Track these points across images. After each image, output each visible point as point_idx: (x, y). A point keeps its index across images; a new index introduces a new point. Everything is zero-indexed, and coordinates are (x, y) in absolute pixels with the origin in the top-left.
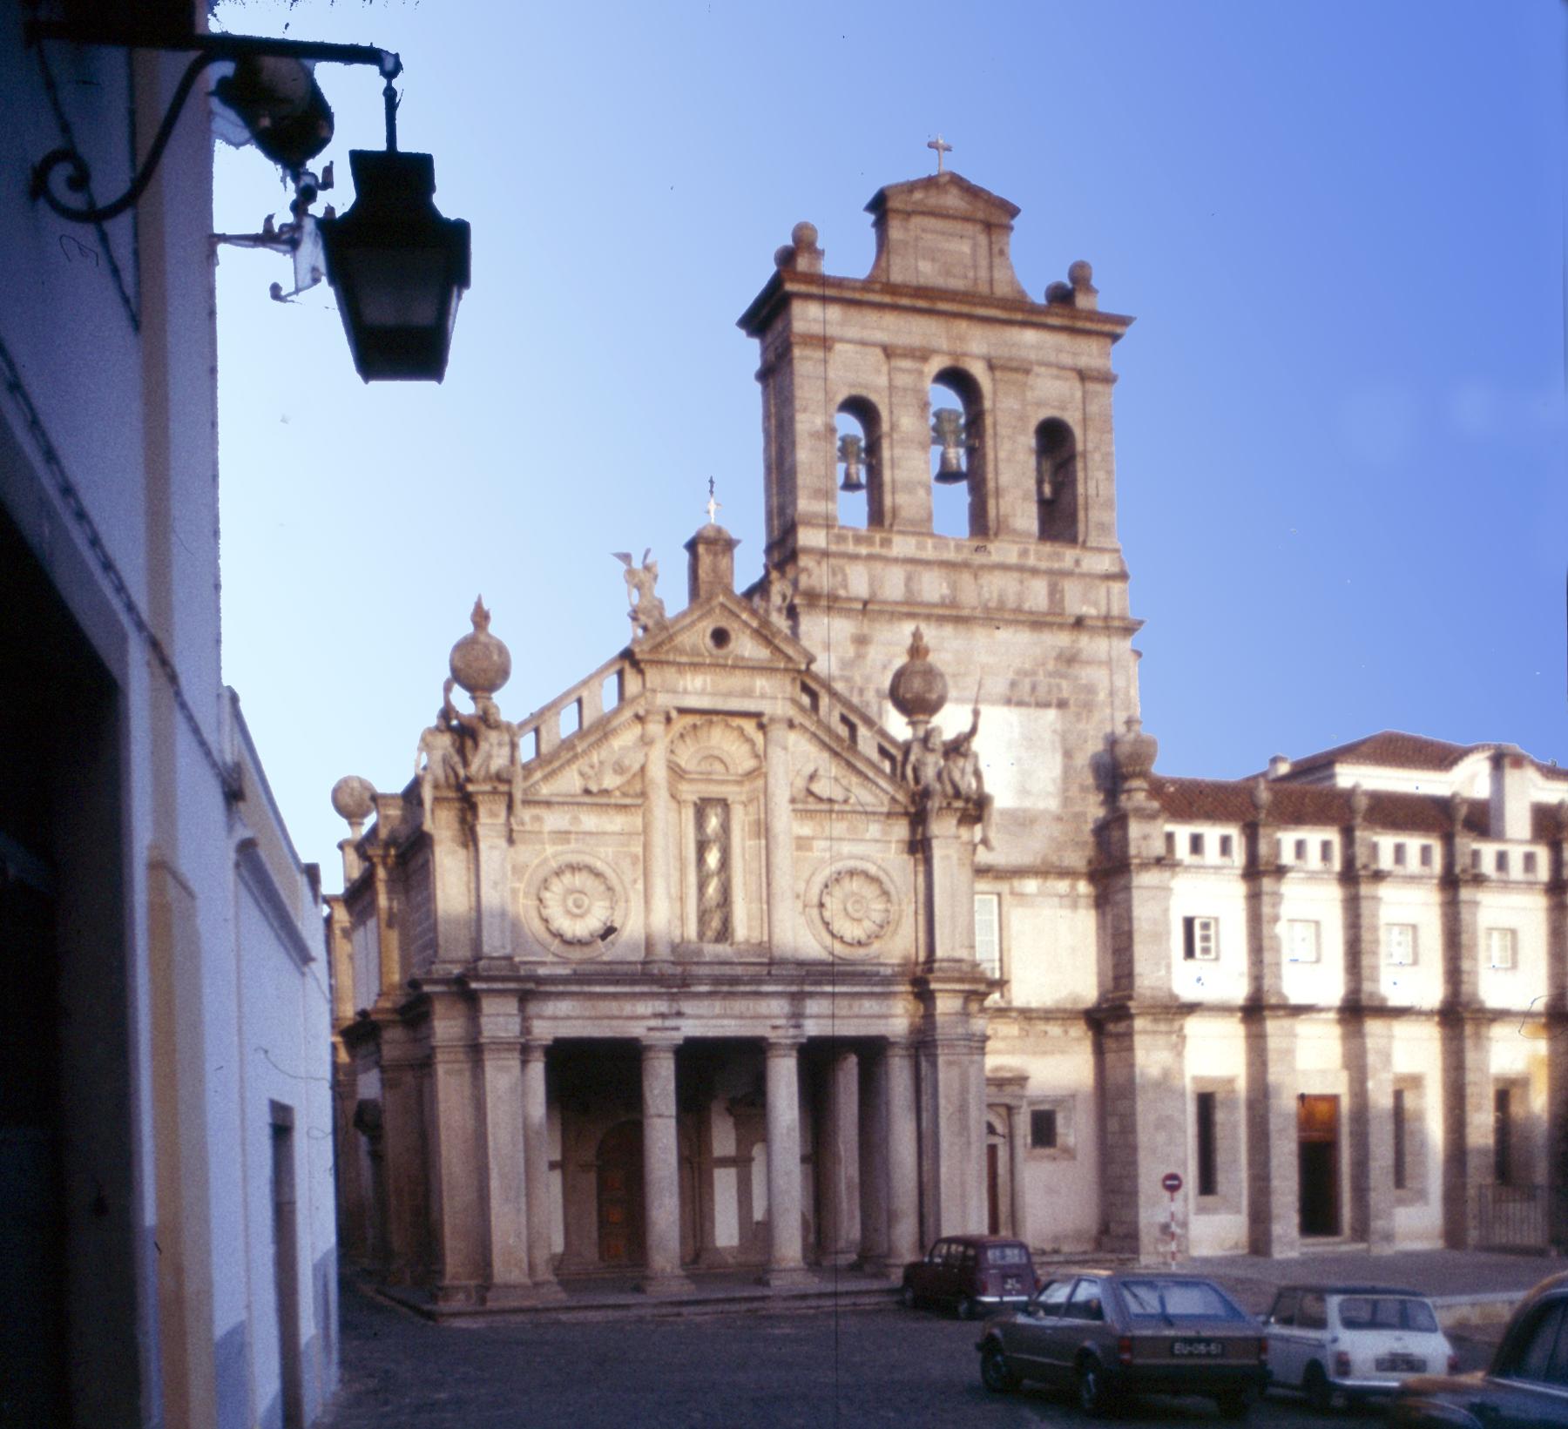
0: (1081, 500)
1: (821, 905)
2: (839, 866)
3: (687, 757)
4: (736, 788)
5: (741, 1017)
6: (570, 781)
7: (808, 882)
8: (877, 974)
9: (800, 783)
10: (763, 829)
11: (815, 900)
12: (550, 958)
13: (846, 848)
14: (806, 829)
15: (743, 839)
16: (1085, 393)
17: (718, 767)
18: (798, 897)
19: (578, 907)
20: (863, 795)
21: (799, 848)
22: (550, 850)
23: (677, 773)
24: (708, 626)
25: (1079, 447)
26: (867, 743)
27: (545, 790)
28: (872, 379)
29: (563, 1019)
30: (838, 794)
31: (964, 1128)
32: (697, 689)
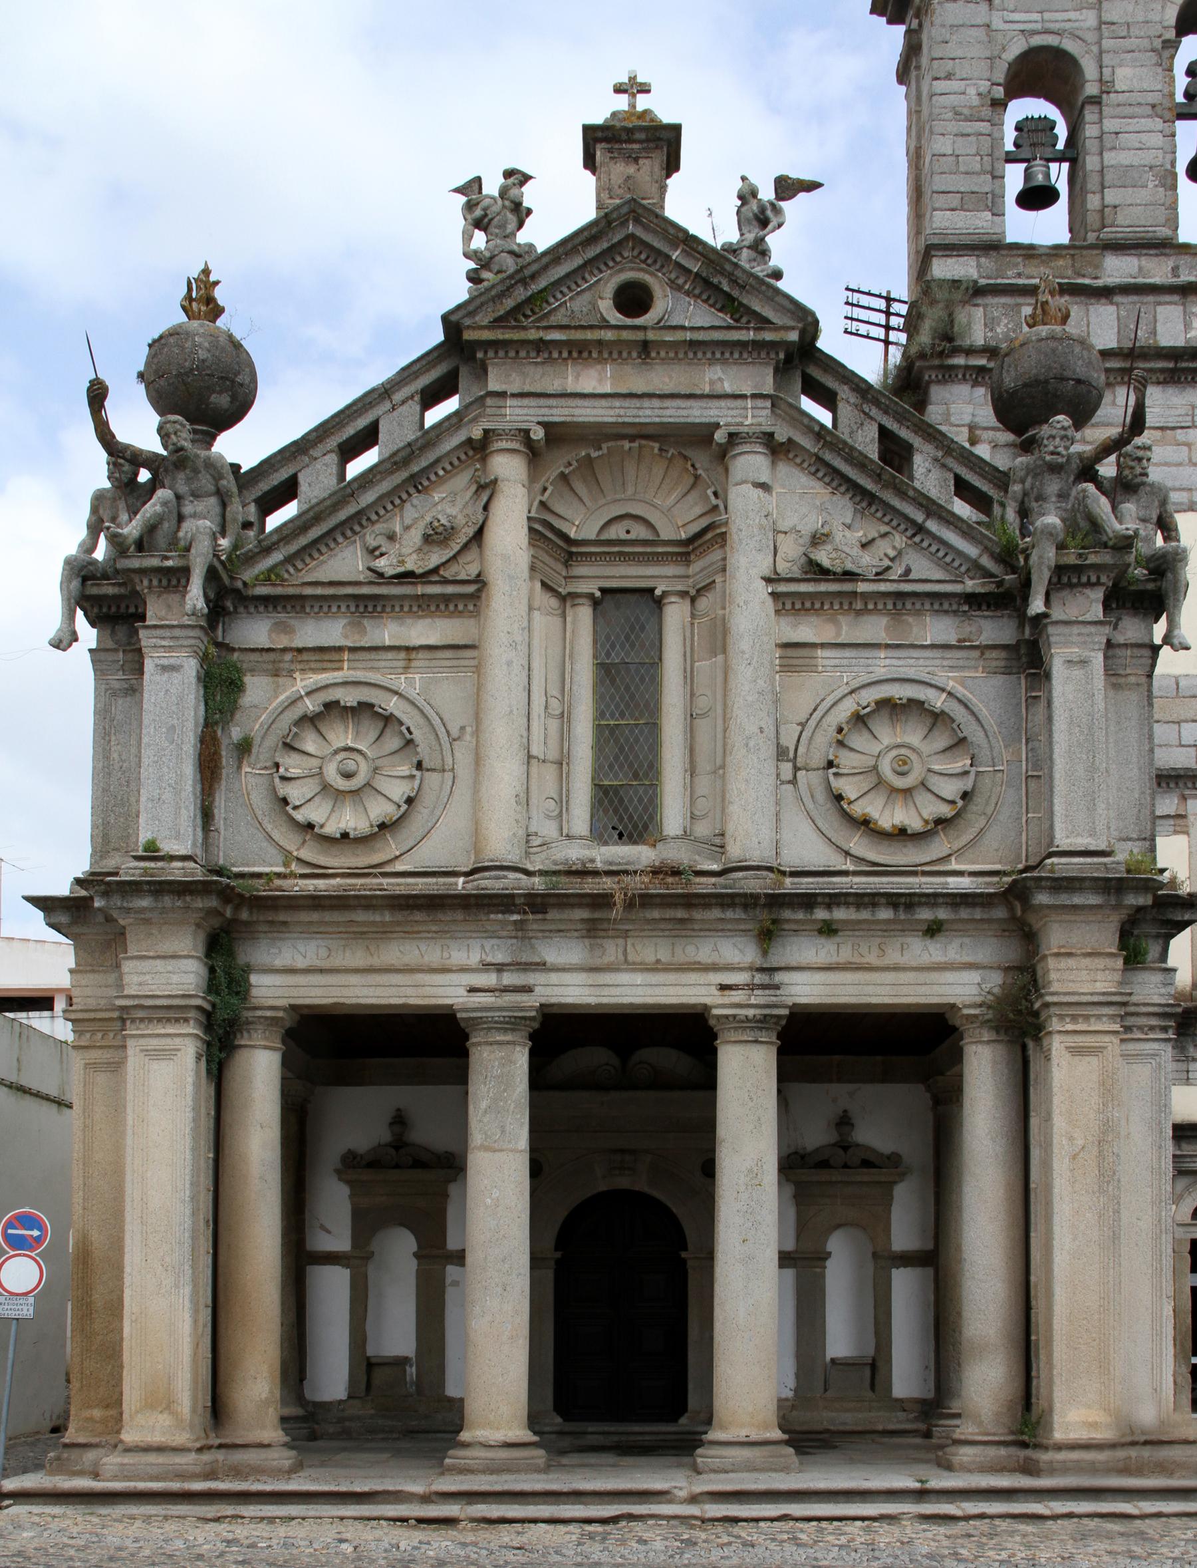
5: (657, 967)
6: (346, 564)
7: (803, 725)
8: (322, 512)
10: (718, 639)
11: (818, 760)
13: (883, 664)
14: (806, 631)
15: (689, 658)
18: (781, 753)
19: (348, 776)
21: (787, 668)
24: (610, 282)
29: (294, 974)
30: (867, 562)
31: (1107, 1178)
32: (593, 390)
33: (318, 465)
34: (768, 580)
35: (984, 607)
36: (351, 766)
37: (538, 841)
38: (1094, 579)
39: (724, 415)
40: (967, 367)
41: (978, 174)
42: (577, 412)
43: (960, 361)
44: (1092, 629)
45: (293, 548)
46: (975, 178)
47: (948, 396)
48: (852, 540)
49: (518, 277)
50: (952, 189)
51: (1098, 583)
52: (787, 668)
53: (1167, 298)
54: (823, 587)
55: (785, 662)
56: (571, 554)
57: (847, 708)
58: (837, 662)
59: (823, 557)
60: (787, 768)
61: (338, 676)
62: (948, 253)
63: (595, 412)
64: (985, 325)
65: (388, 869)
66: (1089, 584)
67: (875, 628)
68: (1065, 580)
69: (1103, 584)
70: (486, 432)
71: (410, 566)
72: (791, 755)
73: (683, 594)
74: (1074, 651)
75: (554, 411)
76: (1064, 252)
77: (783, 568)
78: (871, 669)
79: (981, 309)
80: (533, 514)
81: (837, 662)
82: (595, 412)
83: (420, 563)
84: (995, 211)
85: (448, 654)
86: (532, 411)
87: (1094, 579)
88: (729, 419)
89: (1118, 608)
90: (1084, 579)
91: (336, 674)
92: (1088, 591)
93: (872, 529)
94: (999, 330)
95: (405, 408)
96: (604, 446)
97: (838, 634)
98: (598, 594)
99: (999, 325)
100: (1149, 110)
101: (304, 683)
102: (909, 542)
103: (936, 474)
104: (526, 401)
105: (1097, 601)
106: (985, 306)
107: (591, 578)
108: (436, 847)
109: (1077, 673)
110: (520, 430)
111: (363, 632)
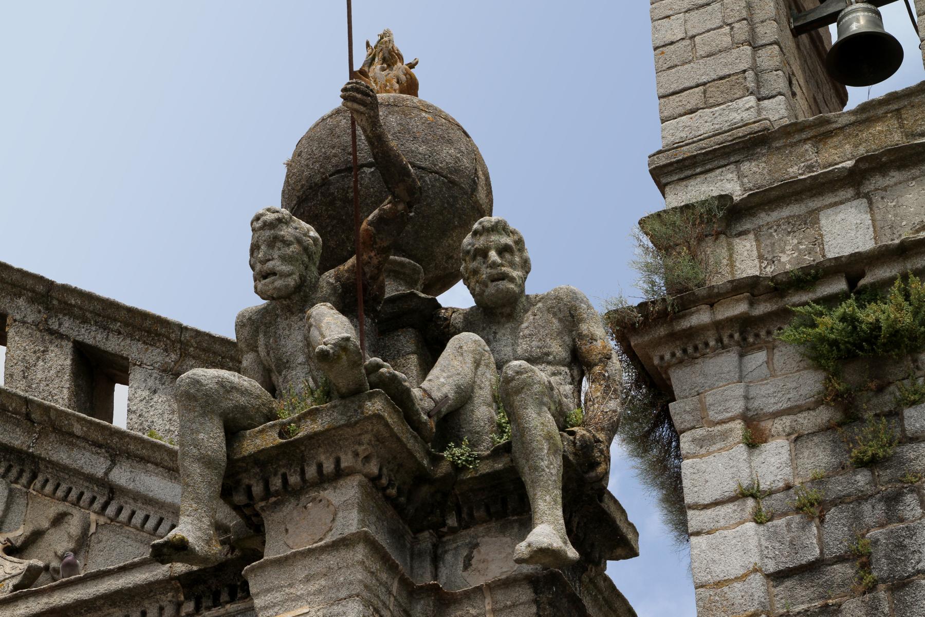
35: (224, 597)
38: (328, 467)
40: (718, 326)
41: (727, 50)
43: (701, 317)
44: (331, 560)
46: (723, 58)
47: (700, 380)
50: (687, 84)
51: (339, 474)
62: (689, 173)
64: (761, 257)
66: (325, 480)
68: (276, 483)
69: (350, 472)
76: (880, 112)
79: (751, 236)
84: (764, 92)
87: (328, 467)
89: (465, 525)
90: (311, 472)
92: (329, 494)
94: (784, 258)
99: (783, 252)
102: (102, 520)
105: (346, 505)
106: (757, 233)
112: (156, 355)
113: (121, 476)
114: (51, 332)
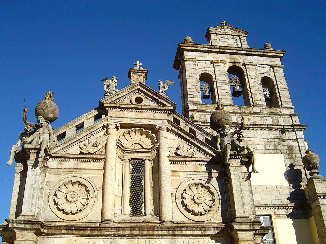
0: (278, 97)
1: (183, 198)
2: (191, 182)
3: (127, 143)
4: (149, 155)
9: (173, 151)
10: (157, 170)
12: (58, 220)
14: (177, 167)
16: (273, 70)
17: (140, 147)
18: (172, 195)
20: (199, 155)
22: (64, 176)
23: (119, 146)
25: (275, 83)
26: (199, 135)
27: (63, 153)
28: (209, 69)
30: (188, 154)
33: (71, 130)
34: (168, 157)
35: (214, 164)
36: (74, 196)
37: (117, 215)
38: (238, 157)
39: (158, 123)
42: (127, 121)
45: (64, 146)
48: (185, 149)
49: (116, 94)
51: (239, 158)
52: (173, 176)
53: (232, 114)
54: (180, 159)
55: (172, 175)
56: (125, 151)
57: (185, 185)
58: (183, 175)
59: (179, 152)
60: (175, 198)
61: (72, 175)
63: (131, 121)
65: (81, 221)
66: (237, 158)
67: (191, 167)
70: (108, 124)
71: (89, 152)
72: (175, 196)
73: (150, 160)
74: (236, 173)
75: (122, 121)
77: (171, 155)
78: (191, 177)
80: (117, 142)
81: (183, 175)
82: (131, 121)
83: (92, 151)
85: (97, 171)
86: (117, 120)
88: (159, 124)
91: (71, 174)
92: (236, 160)
93: (189, 147)
95: (90, 119)
96: (132, 129)
97: (183, 169)
98: (131, 160)
100: (225, 84)
101: (64, 177)
103: (201, 137)
104: (116, 118)
107: (129, 156)
108: (92, 215)
109: (237, 177)
110: (115, 124)
111: (78, 165)
112: (199, 132)
113: (202, 147)
114: (186, 125)
